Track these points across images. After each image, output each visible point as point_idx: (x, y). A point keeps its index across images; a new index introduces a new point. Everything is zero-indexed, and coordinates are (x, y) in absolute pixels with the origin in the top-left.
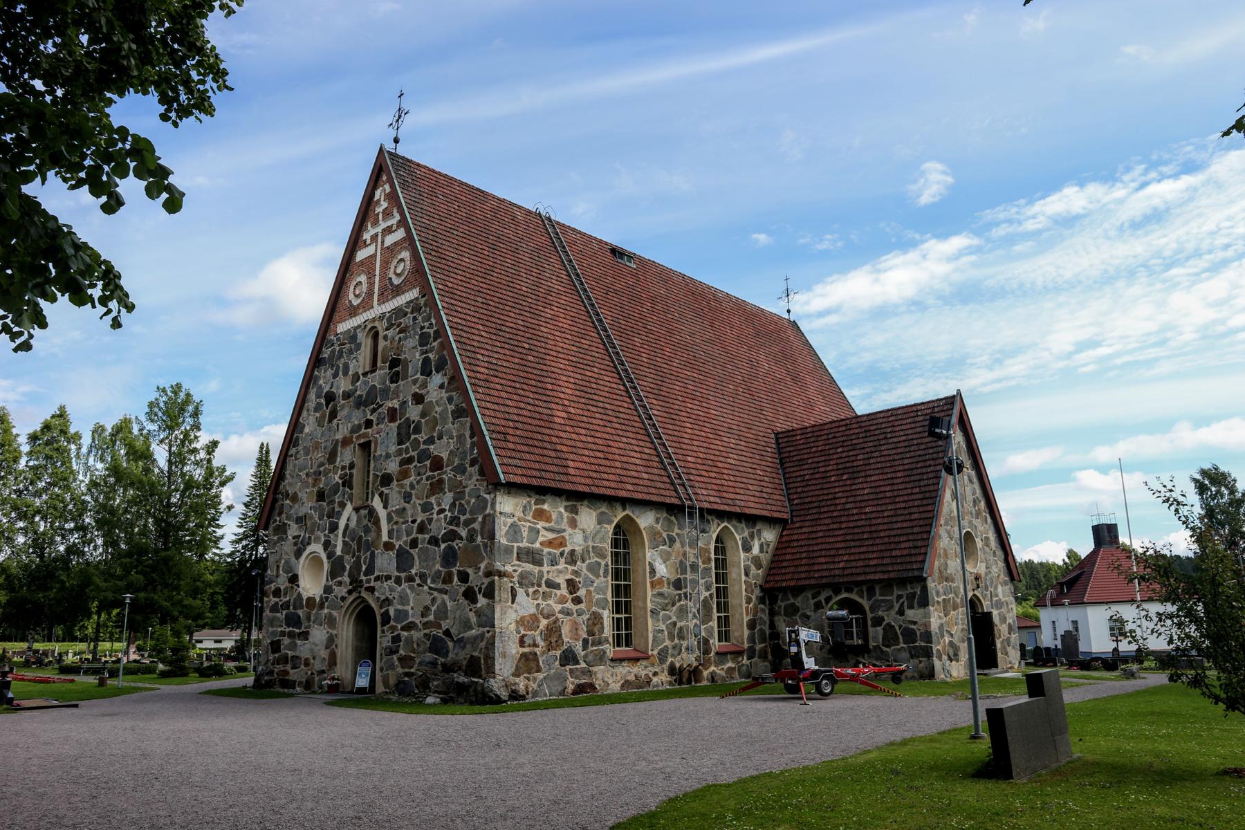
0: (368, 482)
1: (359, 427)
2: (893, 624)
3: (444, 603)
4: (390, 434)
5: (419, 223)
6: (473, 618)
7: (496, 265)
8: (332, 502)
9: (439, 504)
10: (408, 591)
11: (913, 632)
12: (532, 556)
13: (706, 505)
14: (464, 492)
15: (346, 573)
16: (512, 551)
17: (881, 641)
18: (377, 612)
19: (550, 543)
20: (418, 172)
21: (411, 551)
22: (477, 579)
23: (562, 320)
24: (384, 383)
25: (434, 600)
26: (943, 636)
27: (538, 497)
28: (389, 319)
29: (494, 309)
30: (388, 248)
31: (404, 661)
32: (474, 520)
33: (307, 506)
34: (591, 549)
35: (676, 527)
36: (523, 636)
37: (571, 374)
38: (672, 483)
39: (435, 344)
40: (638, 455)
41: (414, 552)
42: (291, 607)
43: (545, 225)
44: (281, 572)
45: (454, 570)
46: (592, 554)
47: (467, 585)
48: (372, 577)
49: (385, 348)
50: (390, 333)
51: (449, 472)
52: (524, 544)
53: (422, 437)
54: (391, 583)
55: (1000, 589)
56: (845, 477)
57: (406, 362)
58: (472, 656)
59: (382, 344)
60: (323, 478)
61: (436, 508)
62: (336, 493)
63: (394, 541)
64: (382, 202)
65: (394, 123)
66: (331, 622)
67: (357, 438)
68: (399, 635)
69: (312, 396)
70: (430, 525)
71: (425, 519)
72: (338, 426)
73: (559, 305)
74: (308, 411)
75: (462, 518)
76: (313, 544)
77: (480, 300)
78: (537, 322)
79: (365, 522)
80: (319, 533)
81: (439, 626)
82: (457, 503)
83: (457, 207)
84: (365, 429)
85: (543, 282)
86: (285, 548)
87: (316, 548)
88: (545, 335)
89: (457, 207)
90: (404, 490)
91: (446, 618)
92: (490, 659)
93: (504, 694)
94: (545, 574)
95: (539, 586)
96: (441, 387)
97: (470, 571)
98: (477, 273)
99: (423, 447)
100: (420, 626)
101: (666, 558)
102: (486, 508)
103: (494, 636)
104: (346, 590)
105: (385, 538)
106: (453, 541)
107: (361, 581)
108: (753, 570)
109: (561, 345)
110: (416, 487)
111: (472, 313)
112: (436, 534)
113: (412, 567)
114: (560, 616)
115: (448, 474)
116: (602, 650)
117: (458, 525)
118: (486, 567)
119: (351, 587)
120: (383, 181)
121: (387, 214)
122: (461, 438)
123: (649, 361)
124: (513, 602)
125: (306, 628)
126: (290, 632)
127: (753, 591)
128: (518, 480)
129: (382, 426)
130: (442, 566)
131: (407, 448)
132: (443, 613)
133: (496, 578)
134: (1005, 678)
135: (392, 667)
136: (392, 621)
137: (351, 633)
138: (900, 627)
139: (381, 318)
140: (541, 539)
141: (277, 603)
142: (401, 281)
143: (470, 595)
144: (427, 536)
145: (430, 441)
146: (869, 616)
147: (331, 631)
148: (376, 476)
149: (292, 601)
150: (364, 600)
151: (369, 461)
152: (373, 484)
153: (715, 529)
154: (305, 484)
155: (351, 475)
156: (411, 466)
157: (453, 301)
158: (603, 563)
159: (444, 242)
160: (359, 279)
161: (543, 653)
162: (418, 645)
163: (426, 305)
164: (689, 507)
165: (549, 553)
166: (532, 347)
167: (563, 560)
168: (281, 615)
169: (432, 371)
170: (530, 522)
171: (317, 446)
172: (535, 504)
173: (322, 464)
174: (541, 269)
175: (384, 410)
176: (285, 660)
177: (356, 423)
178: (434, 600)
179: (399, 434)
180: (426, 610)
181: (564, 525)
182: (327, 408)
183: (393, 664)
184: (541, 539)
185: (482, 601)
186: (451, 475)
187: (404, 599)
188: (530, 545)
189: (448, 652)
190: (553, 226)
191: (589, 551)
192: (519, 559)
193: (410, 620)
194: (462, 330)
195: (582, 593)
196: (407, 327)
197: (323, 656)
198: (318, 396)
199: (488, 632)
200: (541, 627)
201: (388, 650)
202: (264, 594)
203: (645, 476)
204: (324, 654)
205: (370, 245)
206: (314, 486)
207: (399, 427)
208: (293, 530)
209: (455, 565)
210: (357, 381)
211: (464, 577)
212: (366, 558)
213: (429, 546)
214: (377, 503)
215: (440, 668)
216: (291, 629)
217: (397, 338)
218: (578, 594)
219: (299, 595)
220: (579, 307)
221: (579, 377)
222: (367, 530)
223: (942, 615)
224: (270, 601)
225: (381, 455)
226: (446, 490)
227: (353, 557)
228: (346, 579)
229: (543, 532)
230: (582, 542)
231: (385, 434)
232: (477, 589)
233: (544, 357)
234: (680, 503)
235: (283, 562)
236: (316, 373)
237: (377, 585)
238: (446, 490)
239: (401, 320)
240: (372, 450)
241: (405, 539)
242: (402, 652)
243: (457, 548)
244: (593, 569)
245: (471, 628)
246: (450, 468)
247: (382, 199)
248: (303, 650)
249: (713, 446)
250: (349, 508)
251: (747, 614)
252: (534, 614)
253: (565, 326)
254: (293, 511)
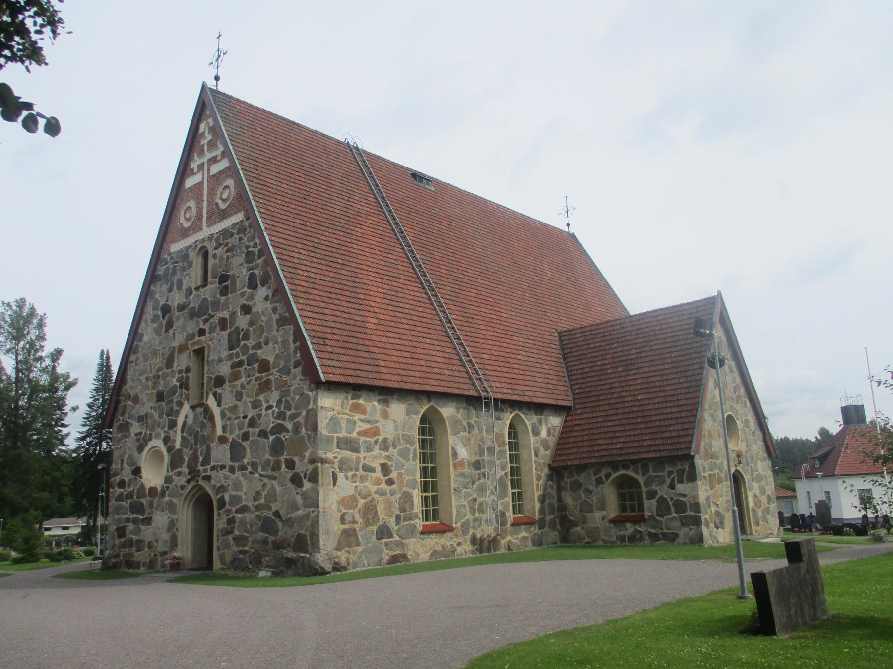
0: (203, 384)
1: (193, 335)
2: (665, 496)
3: (273, 489)
4: (222, 341)
5: (241, 154)
6: (299, 500)
7: (311, 190)
8: (171, 402)
9: (267, 401)
10: (241, 478)
11: (684, 503)
12: (349, 444)
13: (499, 396)
14: (289, 390)
15: (185, 465)
16: (333, 441)
17: (655, 512)
18: (213, 498)
19: (365, 433)
20: (238, 107)
21: (243, 443)
22: (302, 466)
23: (371, 238)
24: (215, 296)
25: (264, 485)
26: (710, 507)
27: (354, 393)
28: (217, 239)
29: (311, 230)
30: (214, 176)
31: (239, 540)
32: (299, 415)
33: (147, 406)
34: (401, 437)
35: (474, 416)
36: (344, 514)
37: (380, 285)
38: (470, 378)
39: (260, 261)
40: (440, 354)
41: (246, 444)
42: (135, 497)
43: (353, 154)
44: (125, 465)
45: (282, 459)
46: (402, 441)
47: (293, 472)
48: (209, 467)
49: (214, 265)
50: (219, 252)
51: (275, 373)
52: (343, 434)
53: (251, 343)
54: (226, 472)
55: (759, 465)
56: (620, 370)
57: (234, 278)
58: (299, 534)
59: (211, 262)
60: (162, 381)
61: (265, 405)
62: (174, 394)
63: (227, 435)
64: (207, 135)
65: (214, 62)
66: (172, 507)
67: (192, 345)
68: (233, 518)
69: (149, 308)
70: (259, 419)
71: (255, 414)
72: (174, 334)
73: (368, 225)
74: (146, 322)
75: (288, 413)
76: (154, 440)
77: (298, 221)
78: (349, 240)
79: (201, 419)
80: (159, 429)
81: (270, 509)
82: (283, 400)
83: (274, 139)
84: (199, 337)
85: (353, 204)
86: (129, 444)
87: (157, 443)
88: (357, 251)
89: (274, 139)
90: (235, 390)
91: (275, 501)
92: (315, 536)
93: (328, 567)
94: (362, 459)
95: (357, 470)
96: (267, 298)
97: (296, 459)
98: (294, 197)
99: (251, 352)
100: (252, 509)
101: (466, 442)
102: (308, 403)
103: (318, 516)
104: (185, 480)
105: (219, 432)
106: (280, 433)
107: (199, 471)
108: (542, 452)
109: (371, 260)
110: (247, 386)
111: (292, 233)
112: (265, 428)
113: (244, 457)
114: (376, 496)
115: (274, 375)
116: (413, 524)
117: (284, 419)
118: (310, 456)
119: (189, 477)
120: (207, 116)
121: (212, 145)
122: (285, 343)
123: (447, 272)
124: (334, 484)
125: (148, 514)
126: (134, 518)
127: (542, 469)
128: (337, 379)
129: (214, 334)
130: (271, 455)
131: (237, 353)
132: (272, 496)
133: (319, 464)
134: (766, 543)
135: (227, 546)
136: (227, 505)
137: (190, 518)
138: (672, 499)
139: (211, 238)
140: (357, 429)
141: (121, 493)
142: (226, 206)
143: (296, 480)
144: (257, 430)
145: (258, 346)
146: (644, 489)
147: (172, 516)
148: (210, 378)
149: (135, 491)
150: (201, 488)
151: (203, 365)
152: (208, 385)
153: (508, 417)
154: (146, 387)
155: (188, 378)
156: (242, 369)
157: (274, 224)
158: (412, 448)
159: (264, 171)
160: (189, 204)
161: (361, 529)
162: (251, 526)
163: (250, 226)
164: (485, 398)
165: (365, 442)
166: (346, 263)
167: (377, 447)
168: (126, 504)
169: (257, 286)
170: (347, 414)
171: (155, 353)
172: (352, 399)
173: (160, 369)
174: (351, 193)
175: (215, 320)
176: (130, 543)
177: (191, 331)
178: (264, 485)
179: (229, 341)
180: (258, 494)
181: (378, 416)
182: (164, 318)
183: (229, 544)
184: (357, 429)
185: (307, 485)
186: (277, 376)
187: (237, 486)
188: (348, 435)
189: (277, 531)
190: (361, 154)
191: (399, 439)
192: (339, 447)
193: (243, 504)
194: (283, 248)
195: (394, 475)
196: (234, 246)
197: (165, 538)
198: (155, 309)
199: (313, 512)
200: (359, 506)
201: (224, 531)
202: (109, 485)
203: (447, 372)
204: (166, 536)
205: (197, 173)
206: (153, 388)
207: (230, 335)
208: (135, 428)
209: (283, 454)
210: (190, 295)
211: (291, 465)
212: (202, 450)
213: (259, 438)
214: (211, 402)
215: (270, 545)
216: (135, 516)
217: (225, 256)
218: (391, 476)
219: (142, 486)
220: (385, 226)
221: (387, 287)
222: (203, 426)
223: (708, 488)
224: (115, 492)
225: (214, 360)
226: (273, 389)
227: (191, 450)
228: (185, 469)
229: (359, 423)
230: (393, 431)
231: (217, 341)
232: (302, 475)
233: (356, 270)
234: (477, 395)
235: (126, 456)
236: (152, 288)
237: (213, 474)
238: (273, 389)
239: (229, 241)
240: (206, 355)
241: (237, 432)
242: (237, 533)
243: (284, 439)
244: (404, 454)
245: (297, 509)
246: (276, 369)
247: (207, 132)
248: (147, 533)
249: (505, 345)
250: (186, 407)
251: (538, 490)
252: (353, 495)
253: (374, 243)
254: (134, 411)
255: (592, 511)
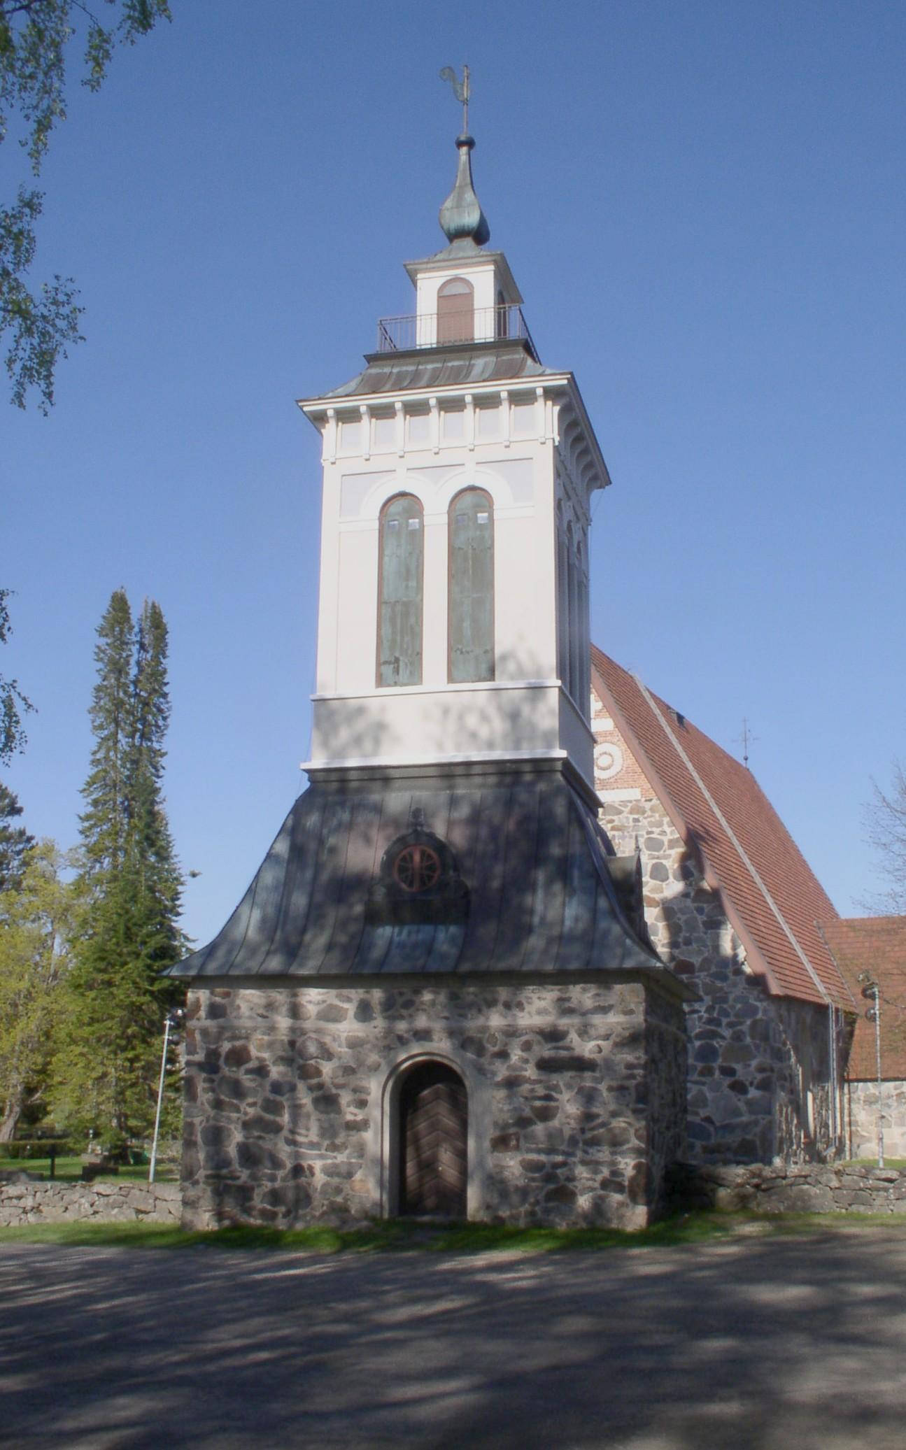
6: (742, 1106)
32: (741, 1023)
51: (702, 977)
75: (725, 1021)
82: (717, 1006)
209: (715, 1060)
232: (747, 1083)
239: (615, 818)
246: (706, 973)
255: (890, 1127)
